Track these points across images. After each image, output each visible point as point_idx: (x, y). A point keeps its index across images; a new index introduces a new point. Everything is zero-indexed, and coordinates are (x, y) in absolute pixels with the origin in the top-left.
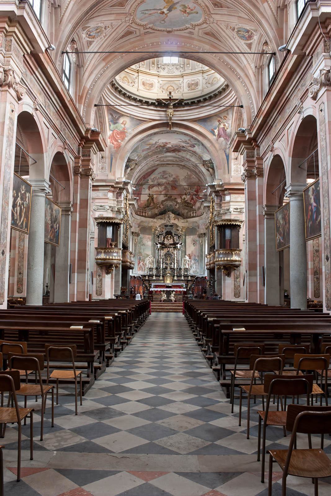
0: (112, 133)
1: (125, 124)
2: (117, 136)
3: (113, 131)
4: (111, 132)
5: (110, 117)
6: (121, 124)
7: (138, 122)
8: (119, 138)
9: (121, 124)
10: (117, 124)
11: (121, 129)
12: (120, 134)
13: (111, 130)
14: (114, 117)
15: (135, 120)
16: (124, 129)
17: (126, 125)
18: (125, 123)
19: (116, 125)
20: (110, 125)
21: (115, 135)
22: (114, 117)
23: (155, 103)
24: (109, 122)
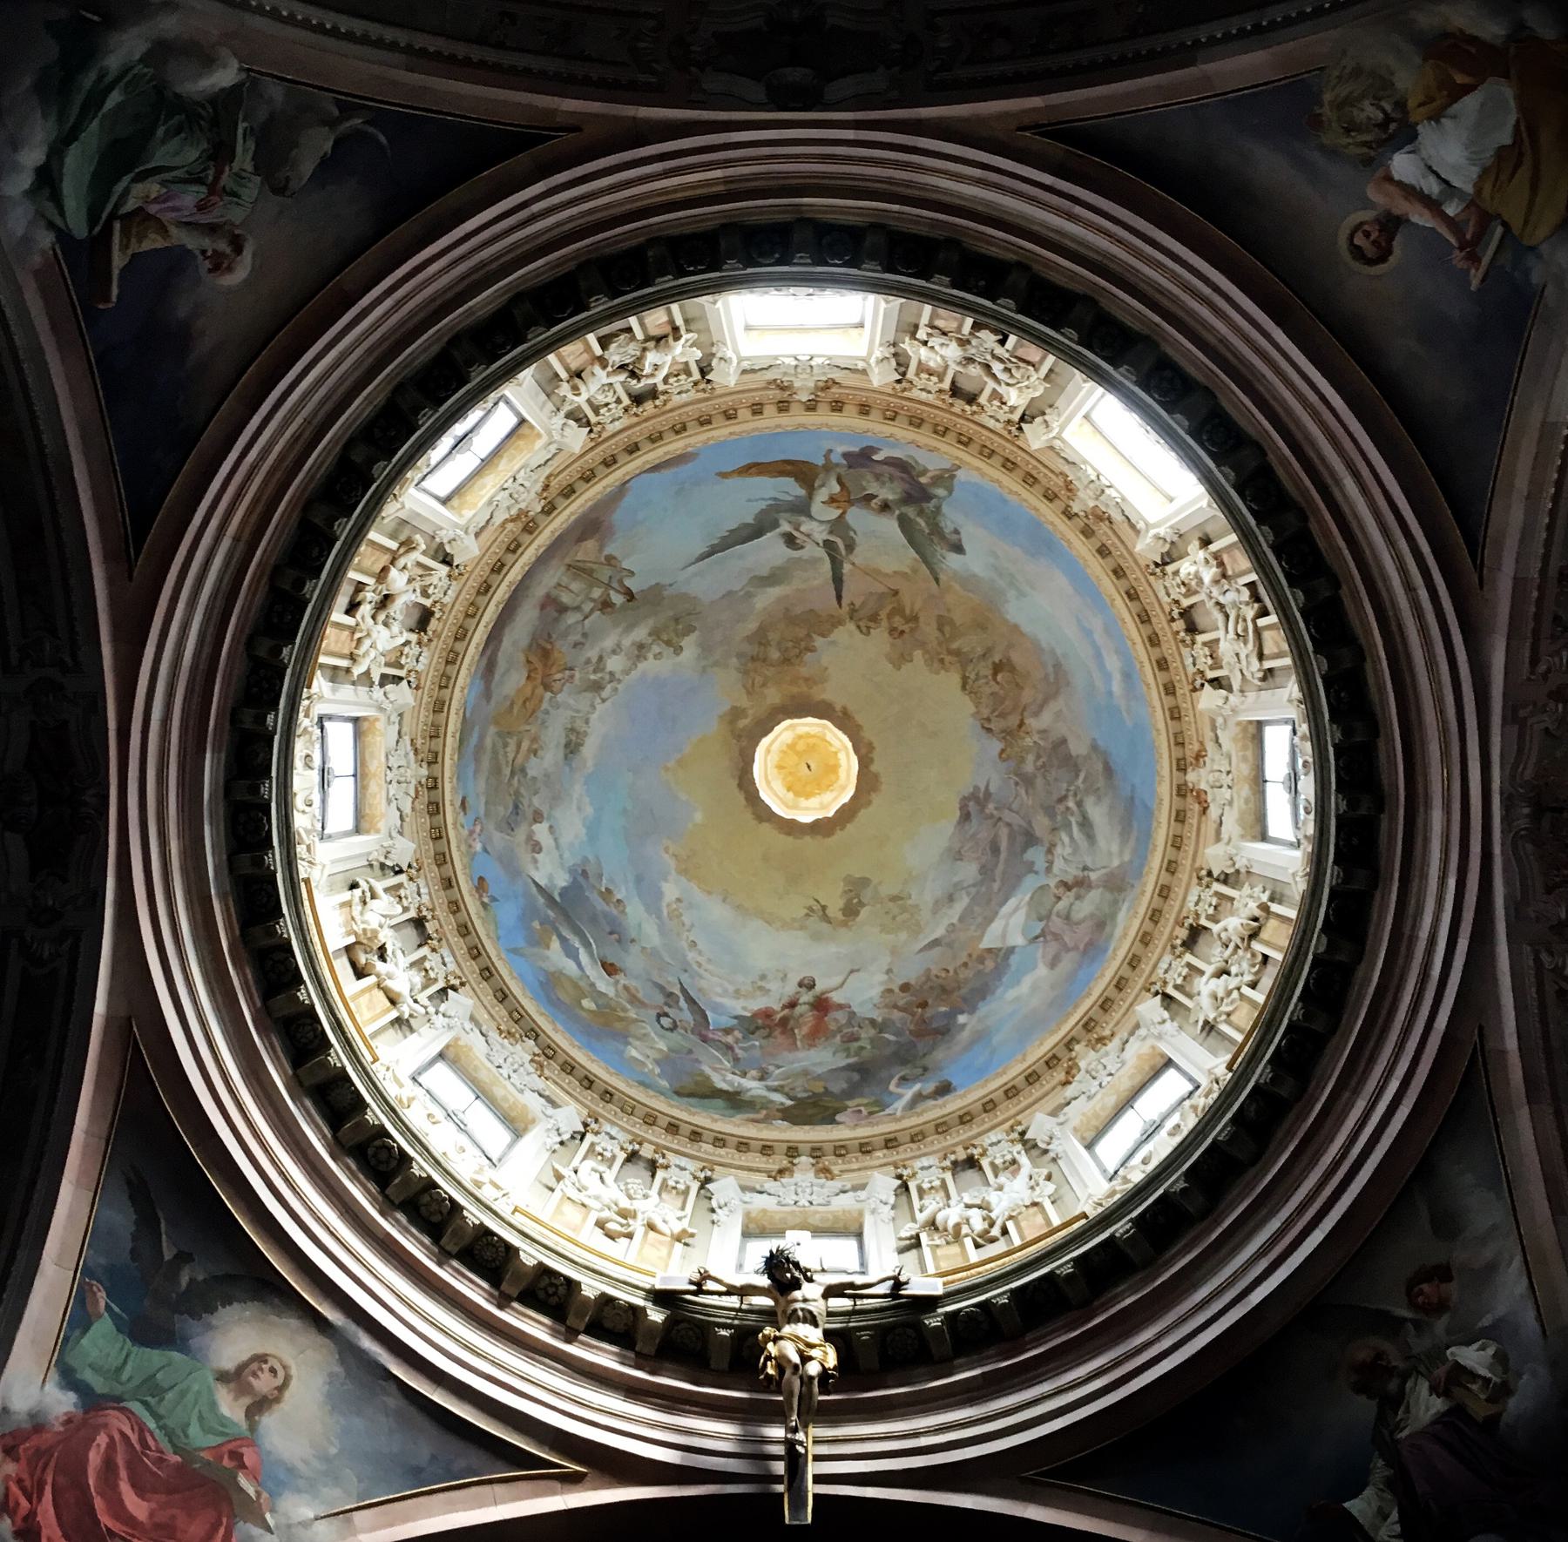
0: (69, 1421)
1: (260, 1405)
2: (125, 1488)
3: (92, 1402)
4: (61, 1403)
5: (123, 1220)
6: (223, 1377)
7: (426, 1445)
8: (130, 1521)
9: (223, 1377)
10: (176, 1356)
11: (197, 1437)
12: (171, 1491)
13: (69, 1379)
14: (168, 1254)
15: (394, 1401)
16: (237, 1456)
17: (269, 1422)
18: (263, 1383)
19: (155, 1357)
20: (78, 1318)
21: (94, 1458)
22: (168, 1254)
23: (634, 1309)
24: (86, 1275)
